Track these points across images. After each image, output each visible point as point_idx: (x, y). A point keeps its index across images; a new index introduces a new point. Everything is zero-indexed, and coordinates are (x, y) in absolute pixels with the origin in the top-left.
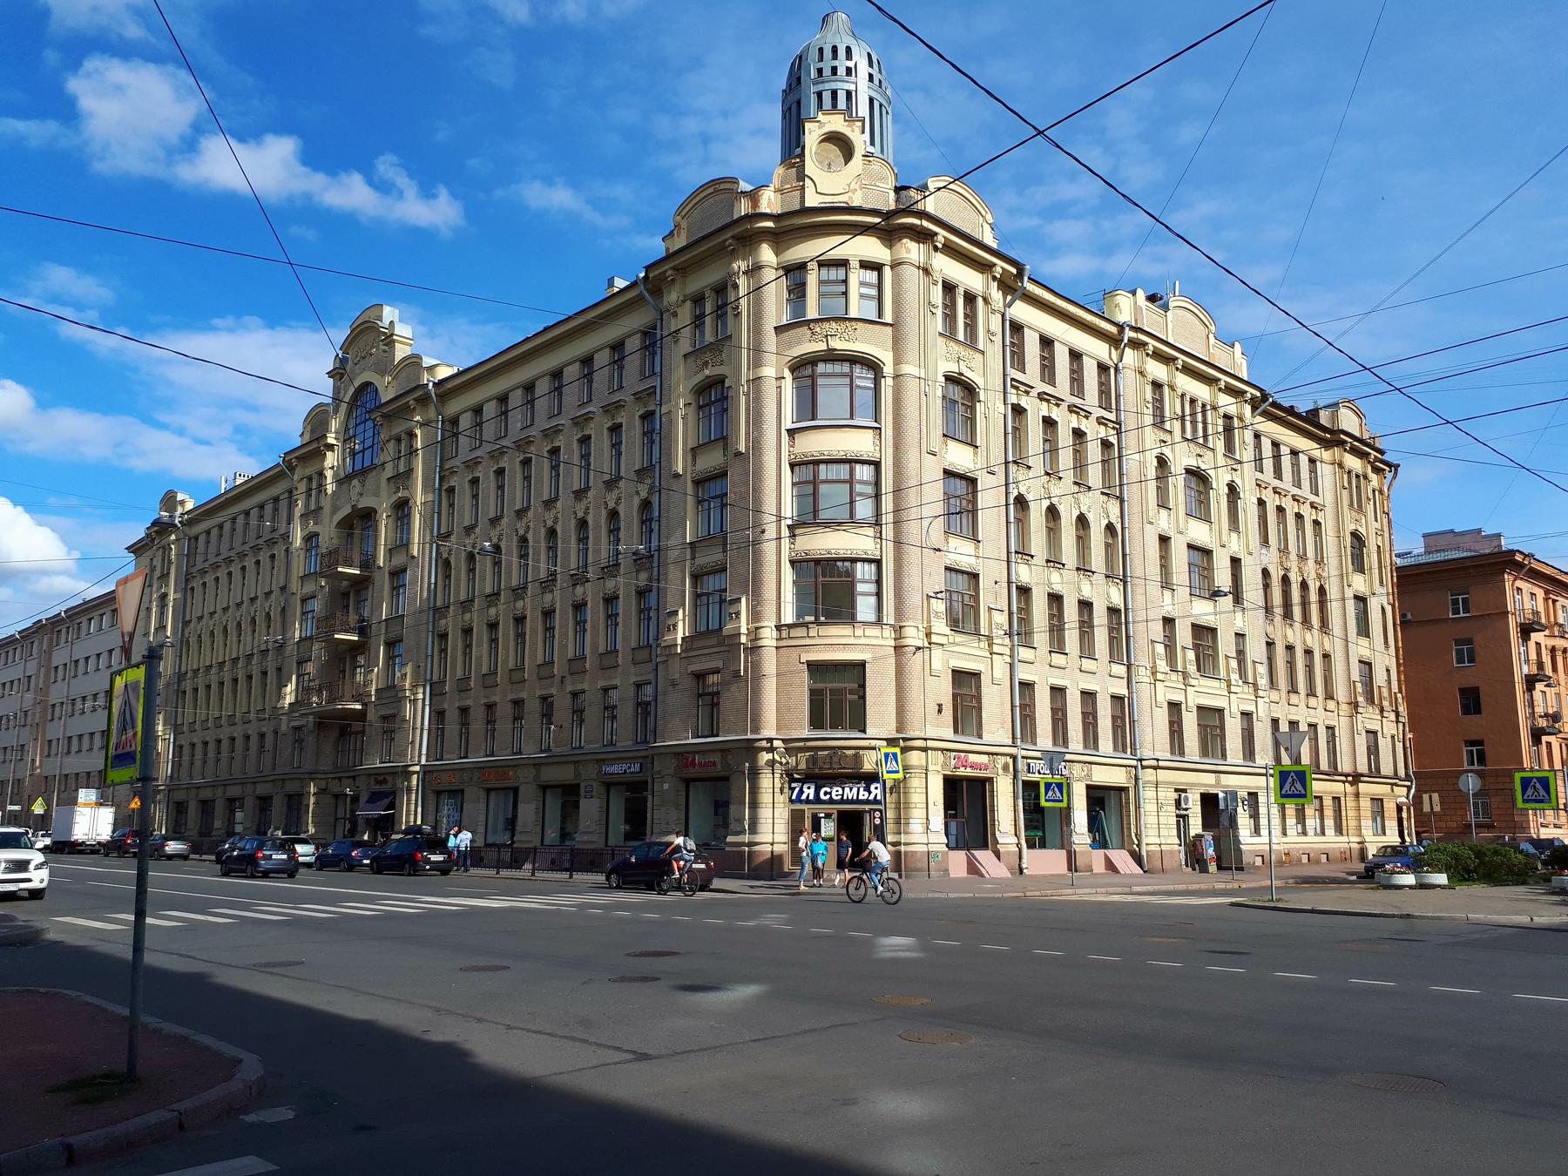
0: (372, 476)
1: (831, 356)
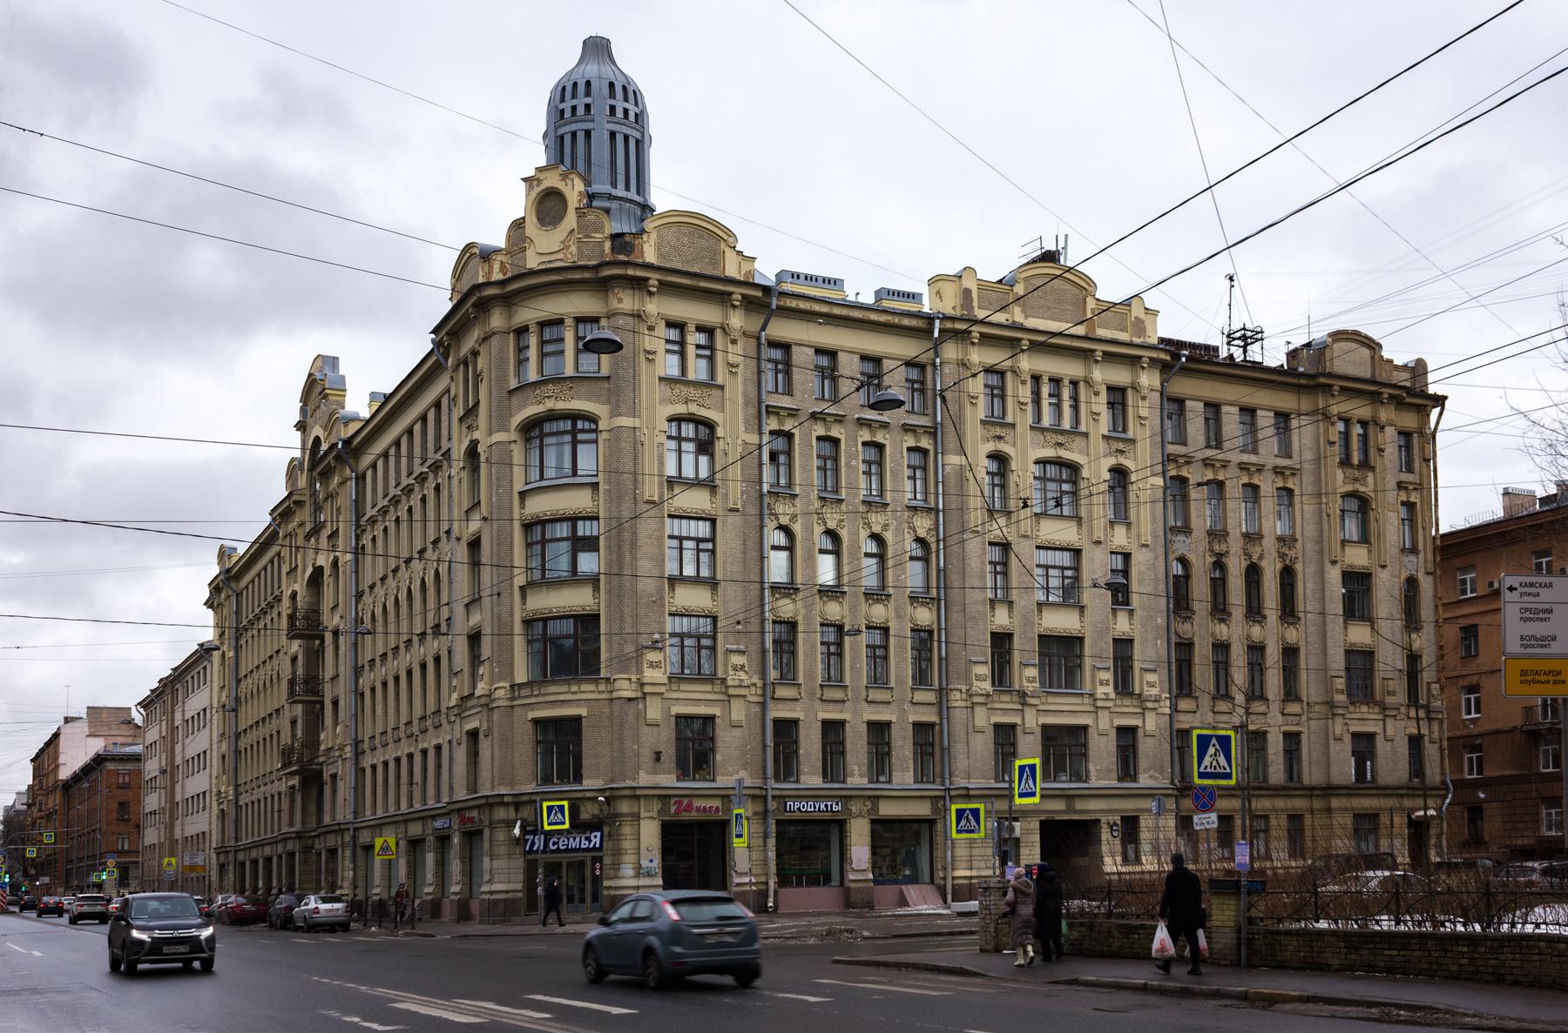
1: (553, 416)
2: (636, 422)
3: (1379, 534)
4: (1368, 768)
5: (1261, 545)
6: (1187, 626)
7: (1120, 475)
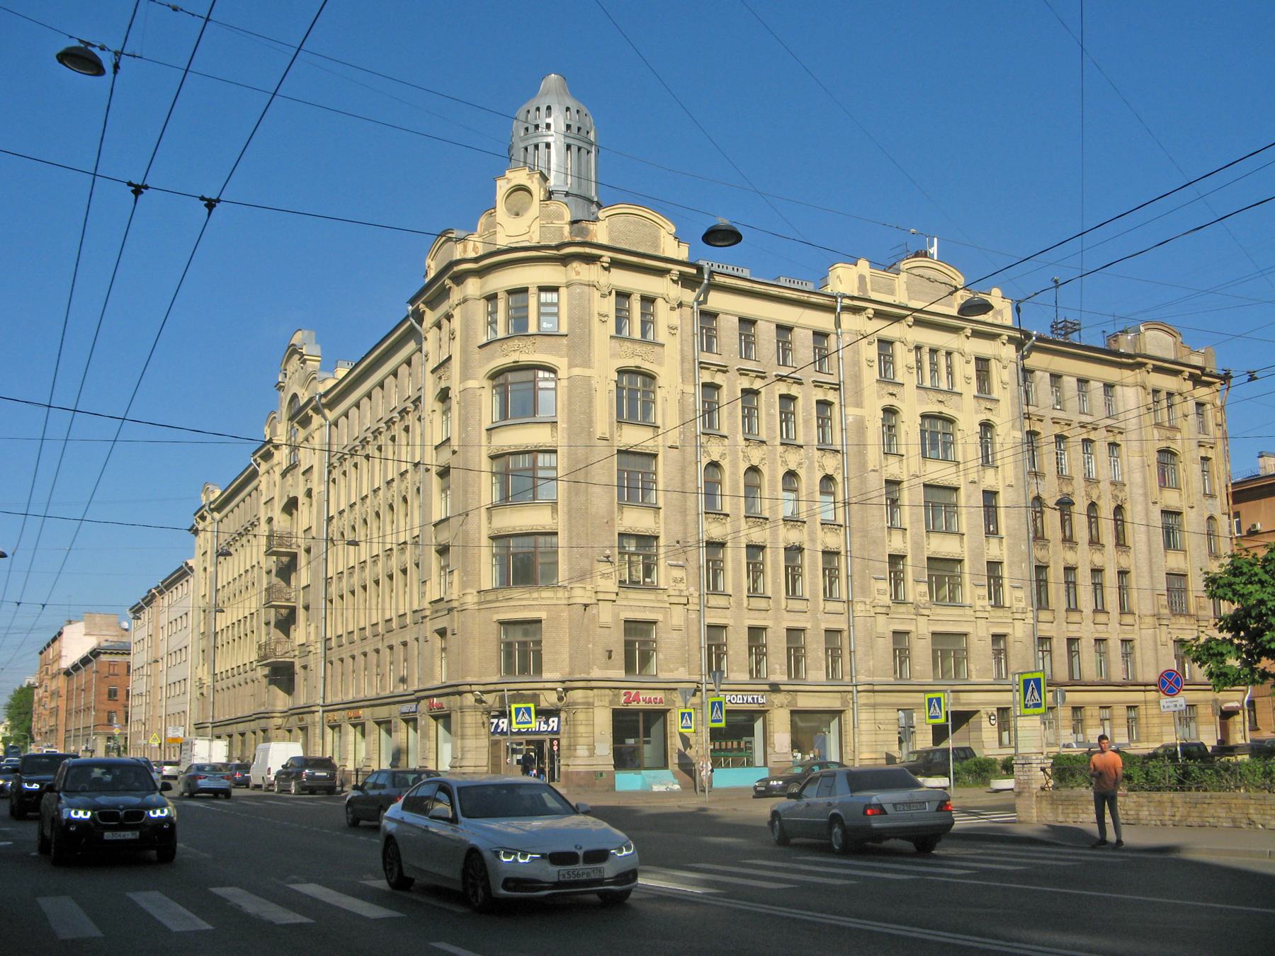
1: (517, 368)
2: (587, 372)
3: (1187, 483)
7: (986, 426)
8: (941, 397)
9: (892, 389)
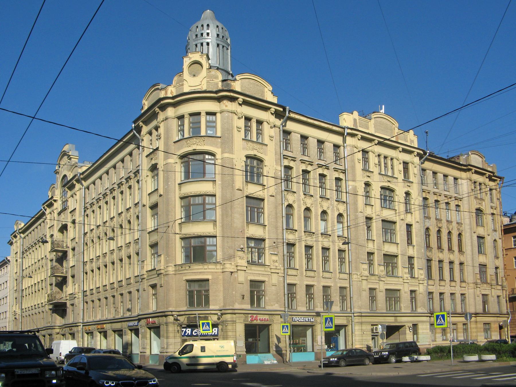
0: (66, 211)
1: (195, 153)
2: (231, 156)
3: (487, 224)
4: (486, 307)
5: (452, 225)
6: (430, 253)
7: (408, 194)
8: (389, 179)
9: (368, 174)
